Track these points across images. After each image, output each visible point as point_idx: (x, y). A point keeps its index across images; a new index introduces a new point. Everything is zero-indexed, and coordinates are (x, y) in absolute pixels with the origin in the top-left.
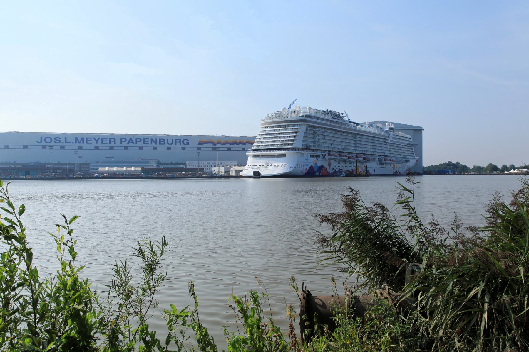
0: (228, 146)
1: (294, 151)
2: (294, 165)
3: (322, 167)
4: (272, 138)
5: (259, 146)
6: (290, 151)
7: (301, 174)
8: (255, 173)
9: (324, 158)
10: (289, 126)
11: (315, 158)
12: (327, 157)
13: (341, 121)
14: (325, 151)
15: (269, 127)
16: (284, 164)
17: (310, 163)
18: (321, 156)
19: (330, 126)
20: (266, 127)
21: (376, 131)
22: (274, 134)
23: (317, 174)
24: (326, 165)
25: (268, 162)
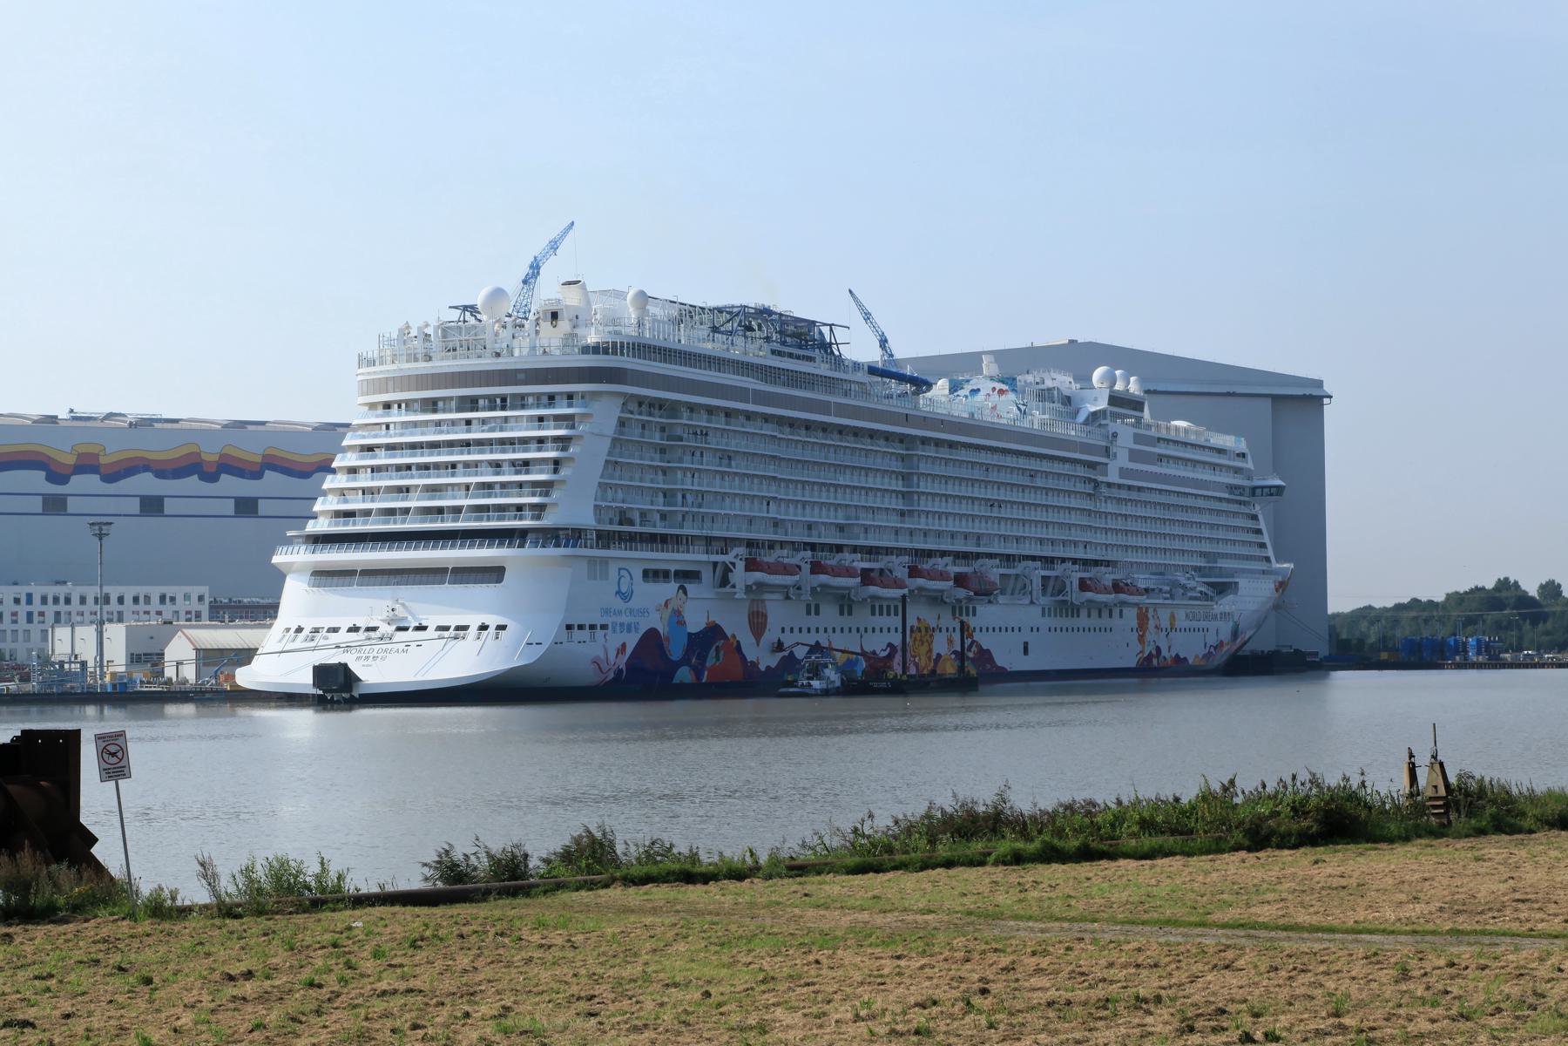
0: (146, 484)
1: (551, 551)
2: (549, 629)
3: (713, 632)
4: (426, 467)
5: (349, 514)
6: (528, 551)
7: (591, 677)
8: (323, 673)
9: (724, 582)
10: (521, 401)
11: (672, 587)
12: (740, 576)
13: (822, 369)
14: (727, 543)
15: (409, 405)
16: (493, 621)
17: (643, 612)
18: (707, 575)
19: (760, 397)
20: (387, 406)
21: (1038, 418)
22: (434, 445)
23: (684, 675)
24: (735, 625)
25: (400, 612)
